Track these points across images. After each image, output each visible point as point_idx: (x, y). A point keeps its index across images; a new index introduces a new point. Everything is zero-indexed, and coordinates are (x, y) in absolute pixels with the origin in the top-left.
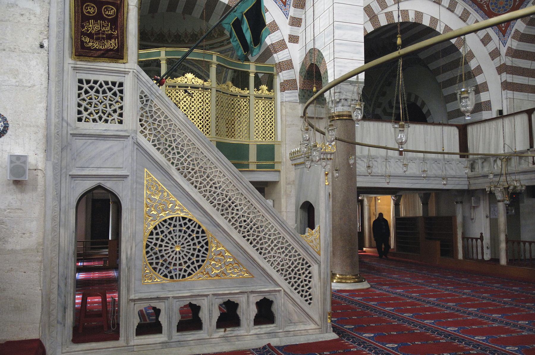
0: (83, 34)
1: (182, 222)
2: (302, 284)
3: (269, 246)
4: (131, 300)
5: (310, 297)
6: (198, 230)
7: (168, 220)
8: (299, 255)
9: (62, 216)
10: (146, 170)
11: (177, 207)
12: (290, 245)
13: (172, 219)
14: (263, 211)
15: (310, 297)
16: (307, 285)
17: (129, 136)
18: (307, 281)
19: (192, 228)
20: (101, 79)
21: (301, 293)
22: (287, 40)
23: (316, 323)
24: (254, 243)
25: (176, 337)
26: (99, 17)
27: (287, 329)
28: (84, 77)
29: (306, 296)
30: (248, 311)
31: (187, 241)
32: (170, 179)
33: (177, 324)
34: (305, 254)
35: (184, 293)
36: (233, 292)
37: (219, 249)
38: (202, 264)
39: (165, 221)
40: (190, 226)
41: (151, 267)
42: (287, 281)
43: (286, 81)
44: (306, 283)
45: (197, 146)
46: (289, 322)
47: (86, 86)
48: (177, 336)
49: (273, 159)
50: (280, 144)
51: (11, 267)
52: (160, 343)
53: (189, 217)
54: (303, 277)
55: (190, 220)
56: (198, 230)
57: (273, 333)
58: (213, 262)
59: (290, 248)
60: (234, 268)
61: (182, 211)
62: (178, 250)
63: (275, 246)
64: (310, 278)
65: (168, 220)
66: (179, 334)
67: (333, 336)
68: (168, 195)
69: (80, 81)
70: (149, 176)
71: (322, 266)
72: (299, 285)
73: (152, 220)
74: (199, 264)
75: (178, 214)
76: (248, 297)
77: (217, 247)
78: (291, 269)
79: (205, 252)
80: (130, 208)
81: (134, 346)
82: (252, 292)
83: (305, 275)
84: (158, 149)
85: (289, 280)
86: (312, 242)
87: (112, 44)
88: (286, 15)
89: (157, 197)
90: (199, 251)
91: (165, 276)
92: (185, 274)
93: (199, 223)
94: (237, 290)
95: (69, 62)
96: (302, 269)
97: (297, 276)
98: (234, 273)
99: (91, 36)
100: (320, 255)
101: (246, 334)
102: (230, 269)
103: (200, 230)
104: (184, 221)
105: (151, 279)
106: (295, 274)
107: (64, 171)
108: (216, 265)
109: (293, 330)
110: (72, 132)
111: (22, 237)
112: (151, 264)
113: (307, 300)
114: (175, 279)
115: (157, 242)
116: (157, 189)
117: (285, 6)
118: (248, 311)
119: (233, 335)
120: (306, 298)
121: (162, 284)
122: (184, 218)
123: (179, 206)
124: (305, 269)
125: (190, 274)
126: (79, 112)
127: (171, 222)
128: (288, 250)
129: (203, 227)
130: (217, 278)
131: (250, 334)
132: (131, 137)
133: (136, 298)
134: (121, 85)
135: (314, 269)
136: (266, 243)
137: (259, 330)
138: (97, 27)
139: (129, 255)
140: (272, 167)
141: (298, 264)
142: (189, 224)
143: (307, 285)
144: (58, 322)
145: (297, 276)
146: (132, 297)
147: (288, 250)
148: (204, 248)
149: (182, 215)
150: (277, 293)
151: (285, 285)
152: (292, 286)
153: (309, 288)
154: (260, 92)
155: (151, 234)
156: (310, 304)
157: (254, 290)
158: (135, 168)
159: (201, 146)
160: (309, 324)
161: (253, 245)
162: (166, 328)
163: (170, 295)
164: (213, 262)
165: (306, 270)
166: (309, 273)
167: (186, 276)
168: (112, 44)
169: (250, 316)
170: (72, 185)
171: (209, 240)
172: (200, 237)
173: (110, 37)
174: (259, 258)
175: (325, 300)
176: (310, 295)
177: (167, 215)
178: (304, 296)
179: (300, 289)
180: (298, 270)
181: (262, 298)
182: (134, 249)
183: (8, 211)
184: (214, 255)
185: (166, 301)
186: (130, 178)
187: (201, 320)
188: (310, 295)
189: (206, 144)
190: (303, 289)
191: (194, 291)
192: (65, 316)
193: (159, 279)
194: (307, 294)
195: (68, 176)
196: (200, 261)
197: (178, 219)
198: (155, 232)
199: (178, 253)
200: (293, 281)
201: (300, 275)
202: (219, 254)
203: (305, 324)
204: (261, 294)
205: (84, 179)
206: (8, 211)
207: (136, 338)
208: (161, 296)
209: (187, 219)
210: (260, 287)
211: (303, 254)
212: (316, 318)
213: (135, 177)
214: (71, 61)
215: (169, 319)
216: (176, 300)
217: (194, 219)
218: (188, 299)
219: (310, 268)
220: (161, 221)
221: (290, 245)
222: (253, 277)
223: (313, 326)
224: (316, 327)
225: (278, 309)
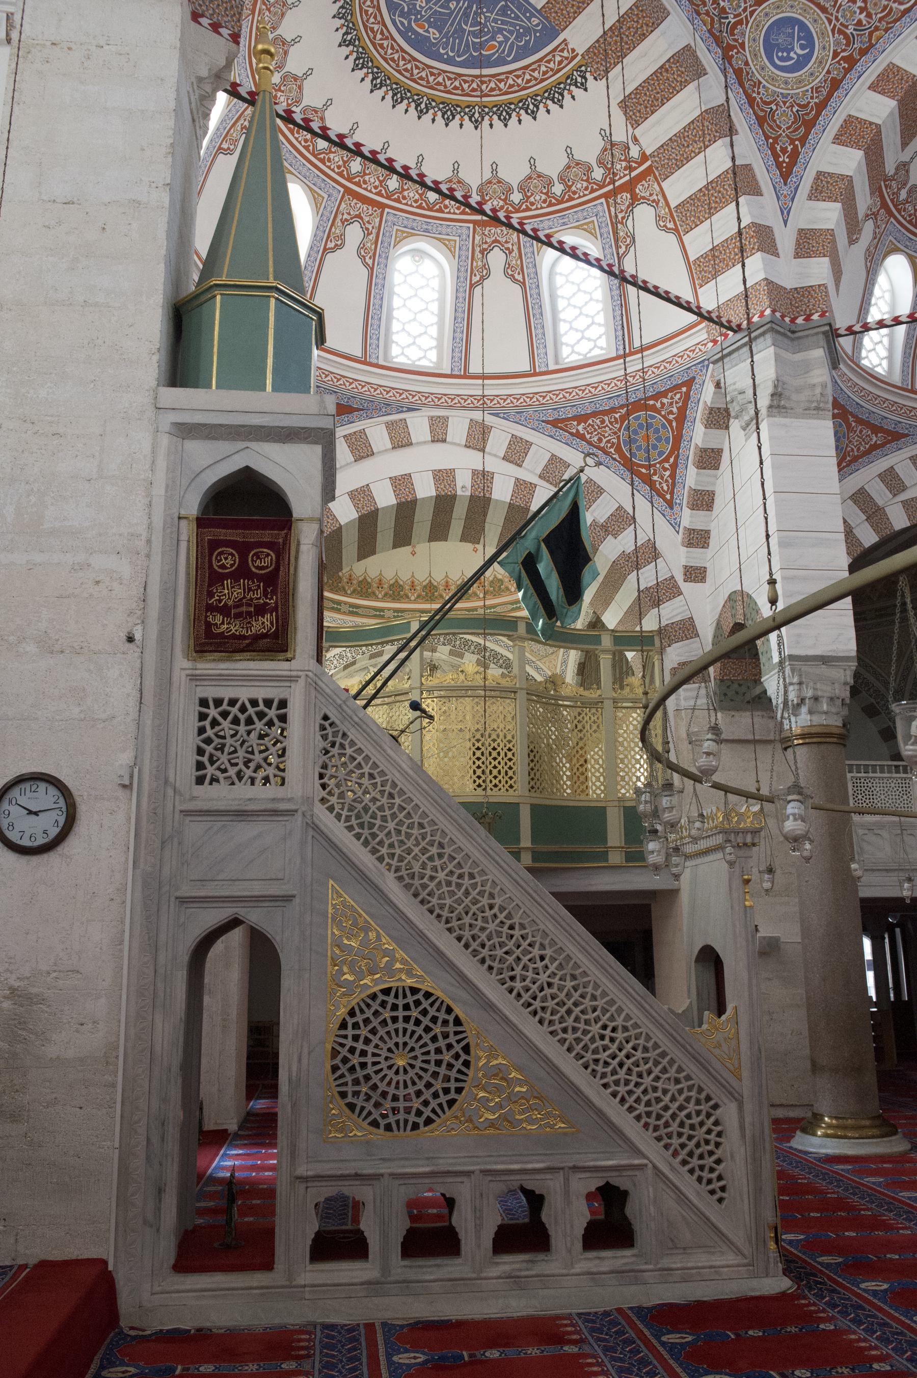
0: (211, 608)
1: (410, 999)
2: (698, 1152)
3: (614, 1057)
4: (297, 1178)
5: (721, 1183)
7: (379, 994)
8: (688, 1078)
9: (160, 986)
10: (331, 882)
11: (398, 965)
12: (663, 1055)
13: (386, 991)
15: (721, 1183)
16: (711, 1153)
17: (296, 811)
18: (712, 1143)
19: (432, 1012)
20: (244, 694)
21: (698, 1173)
23: (739, 1252)
24: (578, 1048)
25: (399, 1270)
26: (242, 572)
27: (666, 1262)
28: (211, 693)
29: (709, 1182)
30: (568, 1216)
31: (422, 1042)
33: (401, 1239)
34: (703, 1077)
36: (530, 1166)
37: (495, 1062)
38: (456, 1096)
39: (374, 997)
40: (429, 1008)
41: (342, 1103)
42: (662, 1143)
44: (709, 1148)
45: (441, 826)
46: (670, 1245)
47: (213, 712)
48: (400, 1268)
51: (54, 1096)
52: (362, 1284)
53: (424, 987)
54: (700, 1133)
55: (428, 995)
56: (447, 1017)
57: (630, 1271)
58: (482, 1094)
59: (665, 1062)
60: (531, 1108)
62: (401, 1063)
64: (719, 1134)
66: (406, 1262)
67: (784, 1284)
68: (378, 938)
69: (204, 703)
70: (337, 896)
71: (748, 1107)
72: (691, 1154)
73: (344, 994)
74: (449, 1097)
75: (400, 979)
76: (567, 1180)
77: (490, 1057)
78: (670, 1112)
79: (464, 1069)
81: (305, 1286)
82: (575, 1169)
83: (704, 1129)
84: (358, 836)
85: (666, 1140)
86: (719, 1046)
87: (264, 624)
88: (675, 526)
91: (375, 1124)
92: (417, 1120)
94: (538, 1162)
95: (182, 664)
96: (698, 1113)
97: (686, 1131)
98: (530, 1121)
99: (225, 611)
100: (740, 1080)
101: (564, 1271)
102: (523, 1112)
103: (451, 1018)
105: (341, 1130)
106: (682, 1125)
107: (165, 889)
108: (488, 1100)
109: (679, 1265)
110: (182, 808)
111: (77, 1031)
112: (343, 1095)
113: (712, 1192)
114: (396, 1132)
115: (355, 1045)
116: (355, 924)
117: (672, 508)
118: (568, 1216)
119: (533, 1273)
120: (710, 1187)
121: (367, 1142)
122: (414, 991)
123: (403, 961)
124: (704, 1113)
125: (429, 1121)
126: (200, 766)
127: (385, 998)
128: (660, 1067)
129: (458, 1010)
130: (492, 1131)
131: (573, 1271)
132: (300, 813)
133: (310, 1173)
134: (283, 704)
135: (729, 1113)
137: (597, 1262)
138: (238, 593)
139: (294, 1074)
141: (687, 1100)
142: (425, 1004)
143: (711, 1153)
144: (145, 1222)
145: (686, 1131)
146: (301, 1171)
147: (660, 1067)
148: (461, 1060)
149: (410, 982)
150: (637, 1173)
151: (654, 1152)
152: (675, 1154)
153: (718, 1162)
155: (343, 1025)
156: (720, 1200)
157: (581, 1164)
159: (450, 827)
160: (722, 1253)
162: (377, 1249)
163: (384, 1169)
164: (482, 1094)
165: (708, 1115)
166: (716, 1123)
167: (421, 1125)
168: (264, 624)
169: (572, 1226)
170: (182, 920)
171: (472, 1041)
172: (451, 1035)
173: (261, 610)
175: (758, 1190)
176: (720, 1178)
177: (376, 982)
178: (705, 1181)
179: (695, 1162)
180: (689, 1116)
181: (601, 1183)
182: (305, 1061)
183: (54, 974)
184: (484, 1076)
185: (374, 1182)
186: (297, 901)
187: (457, 1233)
188: (720, 1178)
189: (461, 822)
190: (701, 1162)
191: (441, 1161)
192: (159, 1209)
193: (359, 1131)
194: (714, 1175)
195: (173, 899)
196: (453, 1090)
197: (400, 991)
198: (350, 1022)
200: (675, 1142)
201: (692, 1127)
202: (496, 1075)
203: (713, 1253)
204: (600, 1175)
205: (206, 905)
206: (54, 974)
207: (309, 1267)
208: (365, 1172)
209: (422, 993)
210: (594, 1156)
211: (700, 1077)
212: (739, 1237)
214: (187, 664)
215: (382, 1226)
216: (397, 1182)
217: (438, 993)
218: (427, 1181)
219: (718, 1112)
220: (363, 995)
221: (663, 1055)
223: (731, 1258)
224: (738, 1260)
225: (640, 1210)
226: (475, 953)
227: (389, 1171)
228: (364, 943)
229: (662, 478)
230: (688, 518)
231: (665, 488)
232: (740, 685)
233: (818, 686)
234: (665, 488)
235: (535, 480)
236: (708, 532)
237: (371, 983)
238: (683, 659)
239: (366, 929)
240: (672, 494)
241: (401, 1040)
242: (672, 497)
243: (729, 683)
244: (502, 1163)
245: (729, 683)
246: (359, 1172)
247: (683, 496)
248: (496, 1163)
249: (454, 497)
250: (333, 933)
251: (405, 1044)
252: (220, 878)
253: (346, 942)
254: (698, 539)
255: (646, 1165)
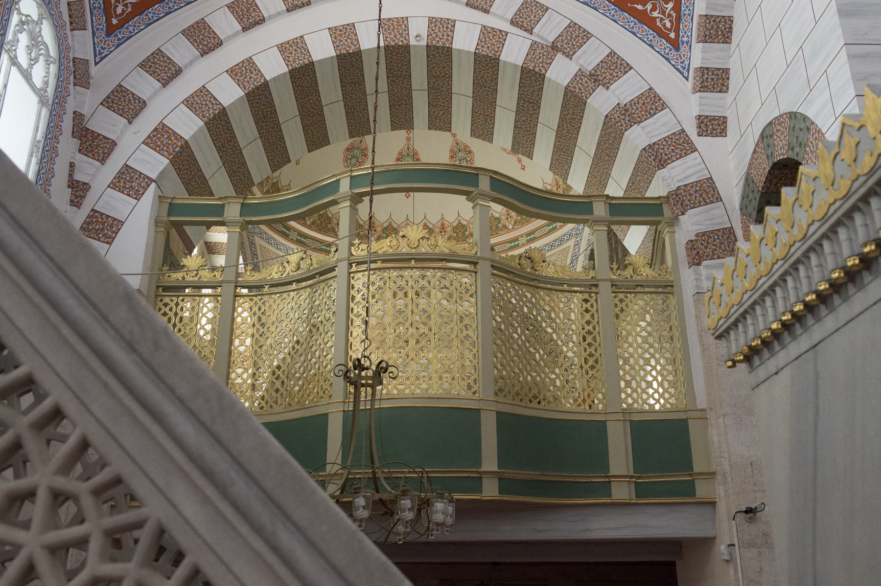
22: (692, 132)
43: (704, 234)
49: (687, 464)
50: (703, 416)
117: (677, 49)
140: (688, 489)
154: (628, 272)
229: (663, 13)
230: (699, 55)
231: (668, 25)
234: (668, 25)
235: (506, 26)
236: (726, 71)
238: (703, 228)
240: (677, 31)
242: (677, 35)
247: (692, 28)
249: (407, 48)
254: (714, 80)
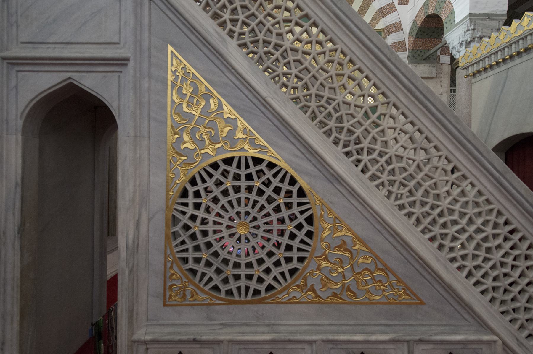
1: (253, 170)
4: (134, 342)
6: (290, 188)
7: (221, 164)
10: (170, 48)
11: (240, 135)
13: (228, 161)
14: (450, 147)
19: (275, 183)
31: (264, 212)
32: (225, 70)
35: (256, 333)
36: (373, 338)
37: (339, 234)
39: (215, 166)
43: (395, 43)
53: (267, 158)
55: (271, 165)
56: (290, 188)
61: (249, 139)
62: (242, 232)
63: (479, 231)
65: (221, 164)
70: (176, 62)
73: (184, 163)
74: (291, 266)
75: (242, 149)
77: (334, 229)
79: (307, 240)
80: (132, 133)
89: (196, 112)
90: (292, 236)
93: (292, 172)
103: (295, 189)
104: (259, 168)
116: (195, 92)
122: (257, 161)
127: (227, 168)
129: (302, 182)
133: (148, 338)
136: (455, 222)
146: (140, 334)
148: (304, 231)
149: (252, 152)
157: (427, 338)
158: (146, 44)
161: (421, 227)
170: (13, 83)
171: (317, 211)
172: (295, 206)
174: (438, 260)
177: (218, 151)
182: (143, 229)
184: (328, 246)
186: (131, 64)
191: (282, 328)
197: (243, 161)
199: (243, 239)
204: (443, 347)
208: (204, 338)
209: (265, 163)
213: (146, 65)
216: (238, 347)
217: (282, 164)
218: (267, 346)
222: (422, 303)
226: (323, 124)
227: (228, 337)
228: (206, 111)
232: (421, 52)
233: (484, 30)
237: (213, 153)
238: (395, 41)
239: (207, 96)
241: (242, 209)
243: (416, 51)
244: (344, 333)
245: (416, 51)
246: (198, 338)
248: (338, 333)
250: (173, 101)
251: (247, 213)
252: (51, 40)
253: (185, 109)
255: (495, 342)
